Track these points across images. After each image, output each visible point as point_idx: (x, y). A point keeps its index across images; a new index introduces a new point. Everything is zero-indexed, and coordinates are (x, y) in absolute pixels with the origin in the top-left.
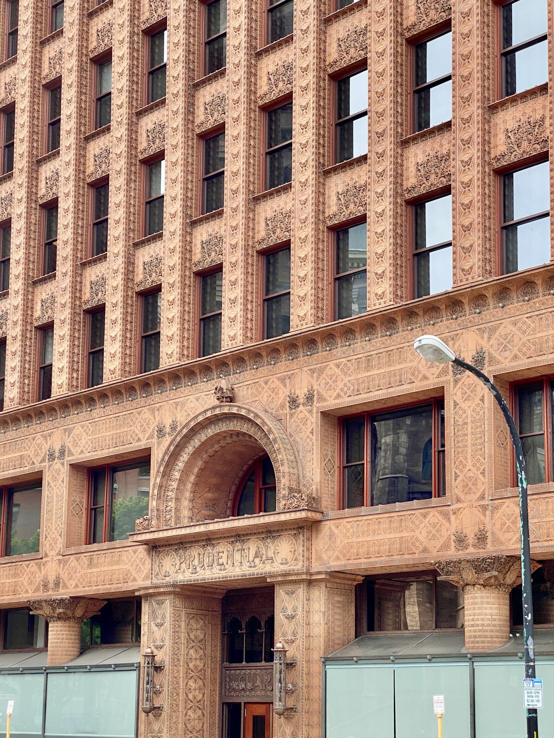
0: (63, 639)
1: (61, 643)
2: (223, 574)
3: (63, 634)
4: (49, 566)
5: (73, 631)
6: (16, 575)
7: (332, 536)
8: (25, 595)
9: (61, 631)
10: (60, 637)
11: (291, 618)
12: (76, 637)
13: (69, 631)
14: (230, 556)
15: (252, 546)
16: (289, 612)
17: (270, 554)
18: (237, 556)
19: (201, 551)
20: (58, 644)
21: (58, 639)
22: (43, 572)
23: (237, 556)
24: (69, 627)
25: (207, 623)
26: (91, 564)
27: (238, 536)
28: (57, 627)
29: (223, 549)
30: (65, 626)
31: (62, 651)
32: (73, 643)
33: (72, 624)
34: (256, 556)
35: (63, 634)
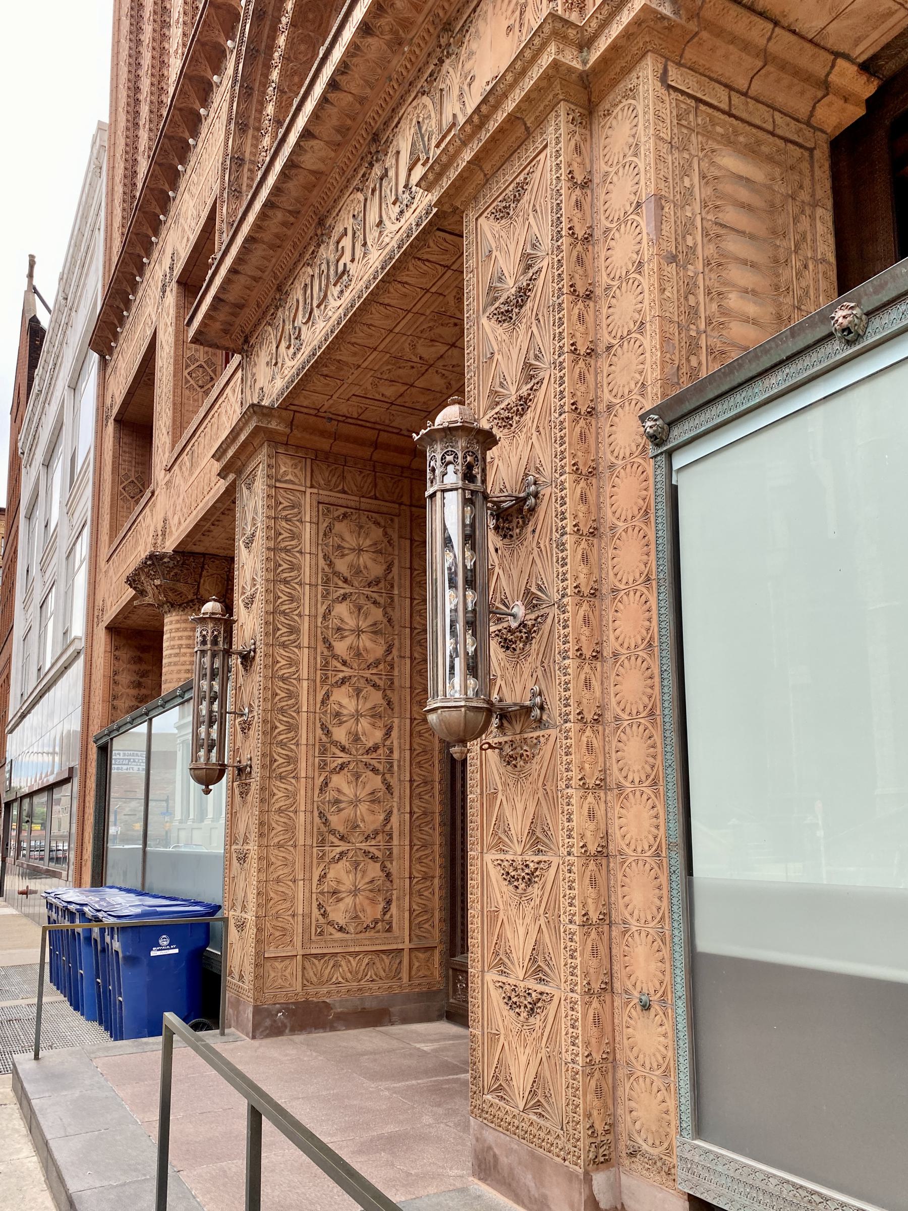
0: (180, 647)
3: (180, 638)
9: (178, 630)
25: (395, 536)
30: (186, 621)
31: (179, 672)
35: (180, 638)
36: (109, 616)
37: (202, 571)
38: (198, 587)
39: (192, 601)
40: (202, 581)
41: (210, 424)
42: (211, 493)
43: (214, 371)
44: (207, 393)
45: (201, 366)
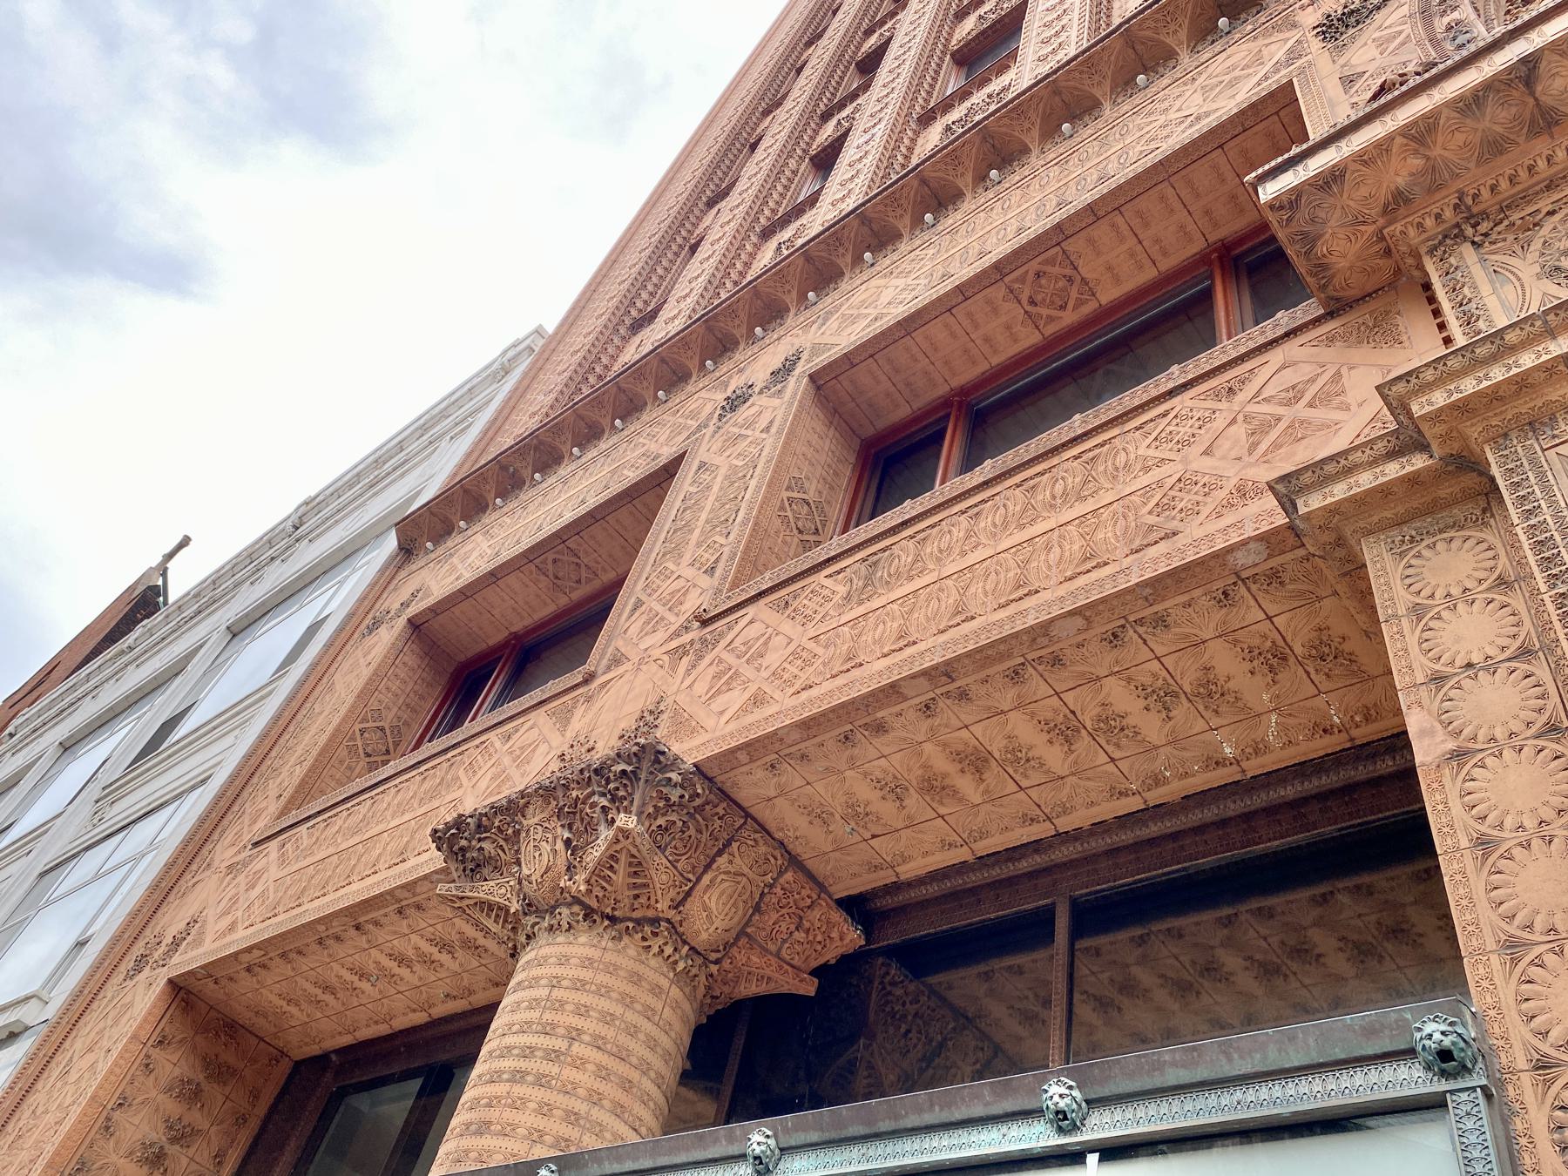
0: (574, 1035)
1: (553, 1055)
3: (582, 1011)
5: (648, 1013)
9: (579, 985)
12: (657, 1063)
13: (627, 1001)
20: (536, 1065)
21: (547, 1030)
24: (636, 979)
28: (563, 960)
32: (627, 1085)
33: (654, 971)
35: (582, 1011)
36: (186, 961)
37: (720, 853)
38: (688, 894)
39: (655, 921)
40: (706, 879)
41: (369, 802)
42: (317, 903)
43: (396, 744)
44: (372, 767)
45: (382, 729)
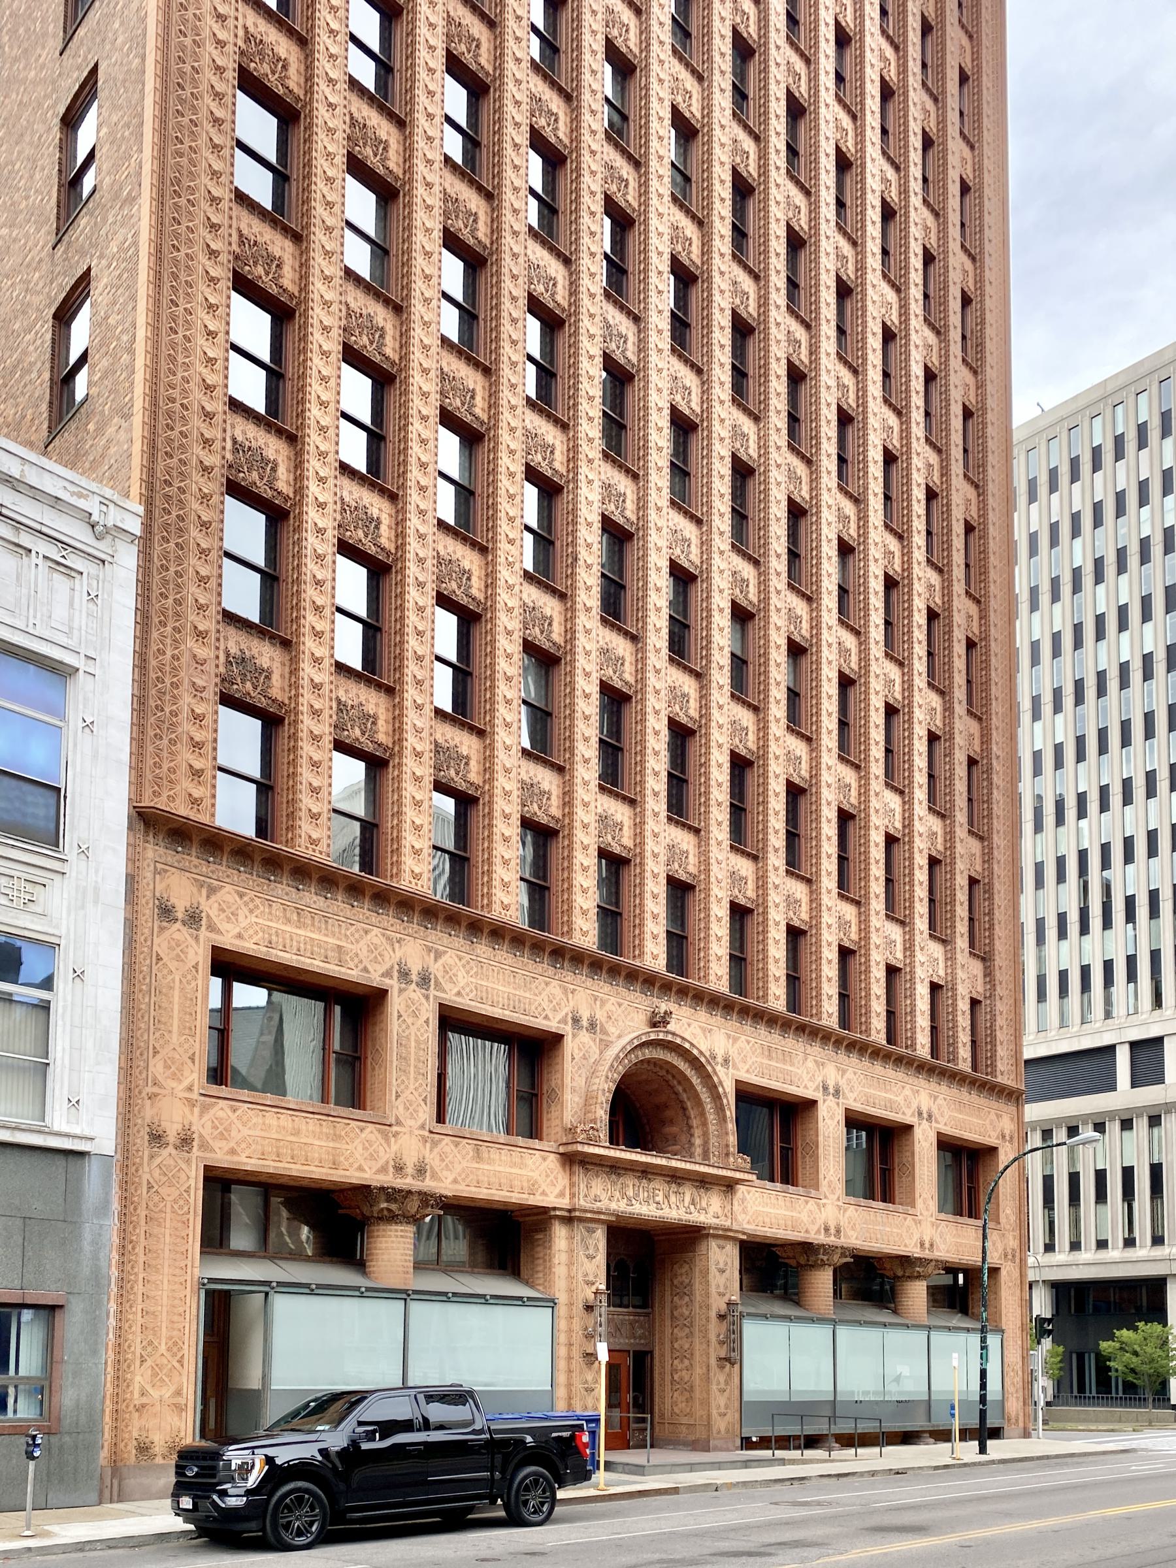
2: (659, 1213)
4: (404, 1140)
6: (337, 1137)
7: (743, 1200)
8: (357, 1174)
10: (822, 1282)
11: (722, 1271)
14: (667, 1197)
15: (688, 1192)
16: (721, 1266)
17: (704, 1204)
18: (673, 1198)
19: (636, 1182)
22: (394, 1148)
23: (673, 1198)
26: (478, 1156)
27: (646, 1172)
29: (659, 1185)
34: (693, 1203)
